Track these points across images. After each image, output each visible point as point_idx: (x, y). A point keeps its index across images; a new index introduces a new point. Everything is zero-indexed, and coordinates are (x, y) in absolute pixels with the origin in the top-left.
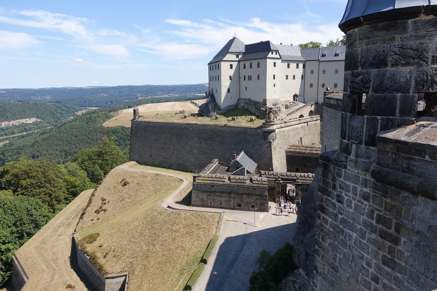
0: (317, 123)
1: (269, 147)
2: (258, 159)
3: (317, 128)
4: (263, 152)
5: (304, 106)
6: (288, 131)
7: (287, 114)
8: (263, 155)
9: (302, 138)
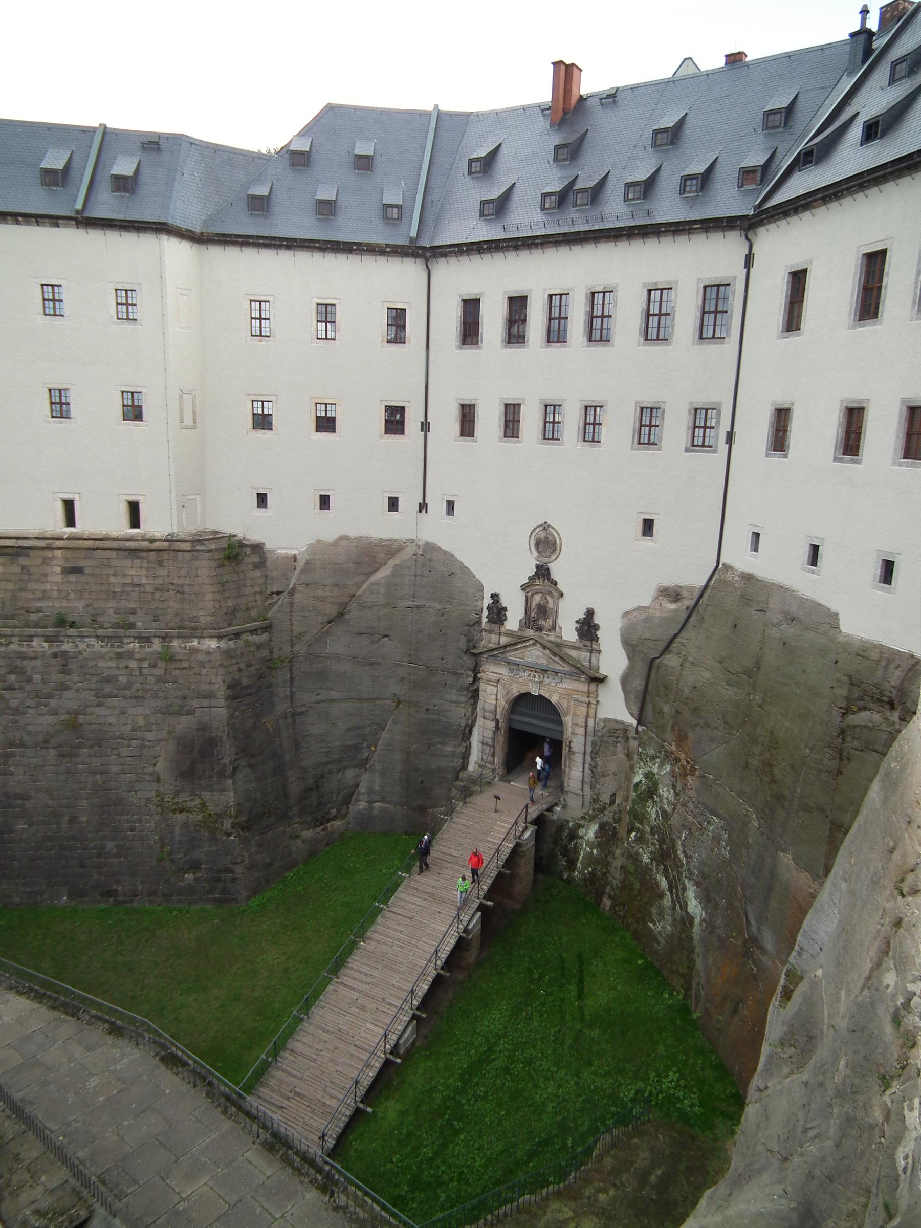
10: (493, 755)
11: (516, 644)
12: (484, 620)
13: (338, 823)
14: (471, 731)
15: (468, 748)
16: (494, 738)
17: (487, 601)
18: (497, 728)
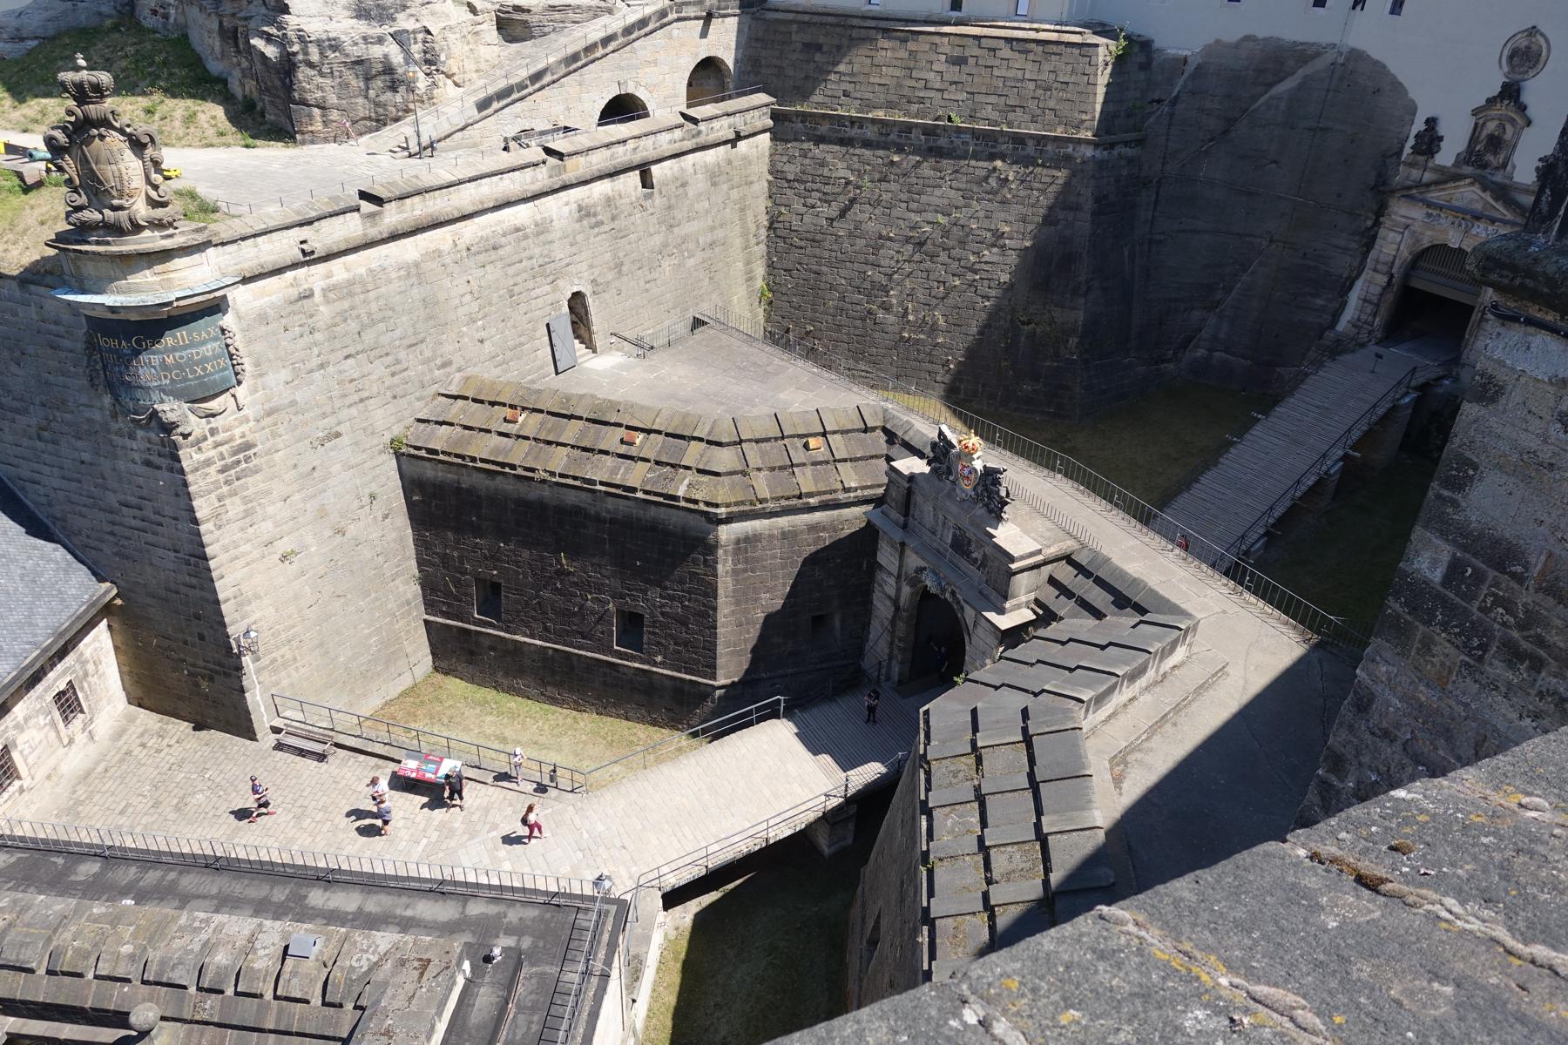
0: (745, 158)
1: (164, 462)
2: (107, 549)
3: (743, 198)
4: (133, 500)
5: (643, 23)
6: (414, 271)
7: (482, 95)
8: (137, 523)
9: (590, 300)
10: (1375, 315)
11: (1446, 182)
12: (1407, 150)
13: (1171, 366)
14: (1352, 284)
15: (1344, 304)
16: (1381, 295)
17: (1419, 126)
18: (1389, 283)
